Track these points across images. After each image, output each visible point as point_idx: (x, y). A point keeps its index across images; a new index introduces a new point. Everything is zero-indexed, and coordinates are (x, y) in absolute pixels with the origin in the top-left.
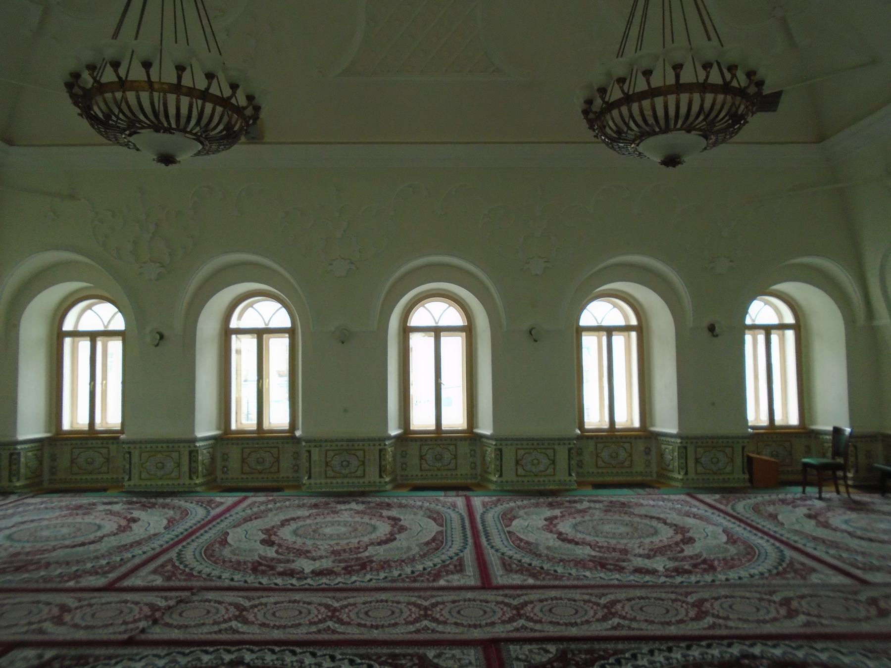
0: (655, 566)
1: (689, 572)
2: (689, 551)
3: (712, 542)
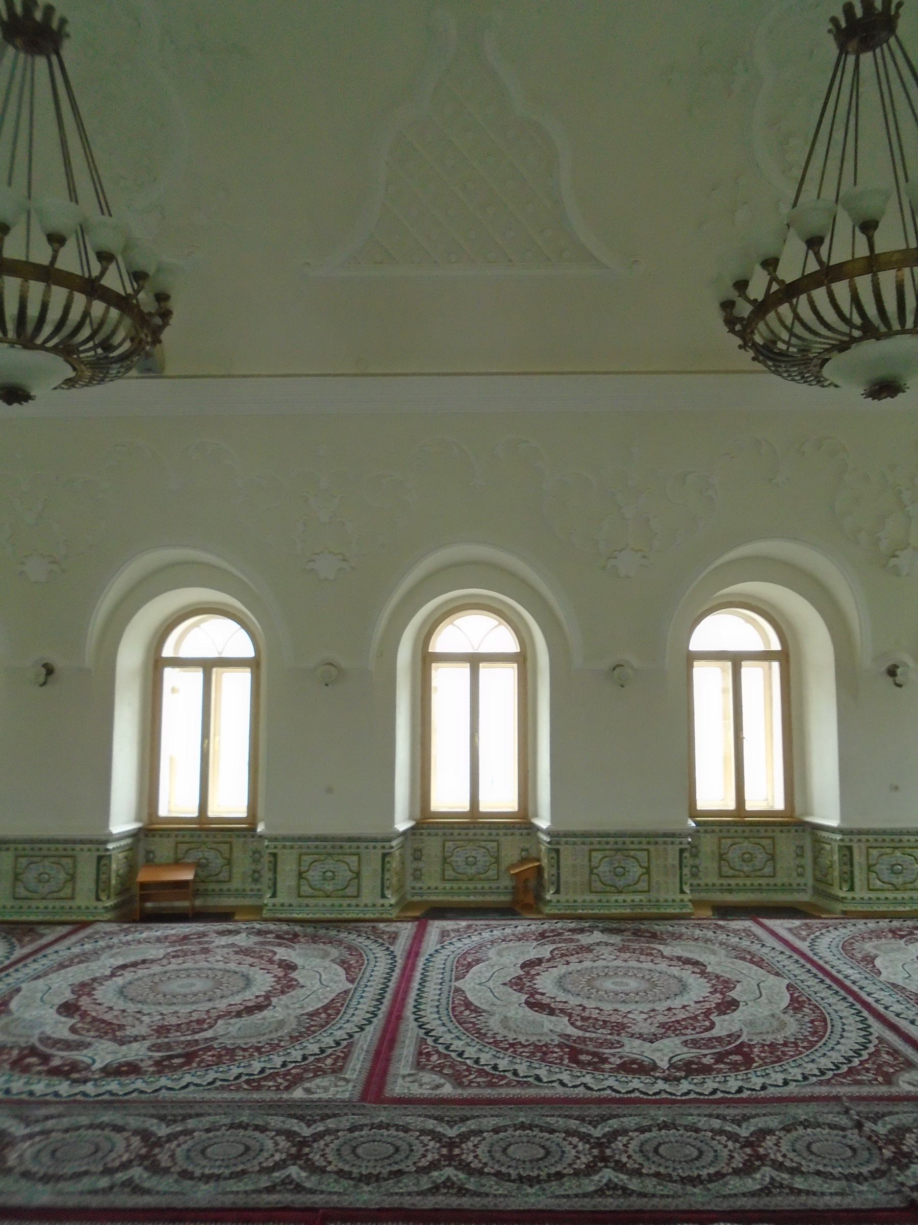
0: (656, 1057)
1: (706, 1070)
2: (723, 1025)
3: (762, 1011)
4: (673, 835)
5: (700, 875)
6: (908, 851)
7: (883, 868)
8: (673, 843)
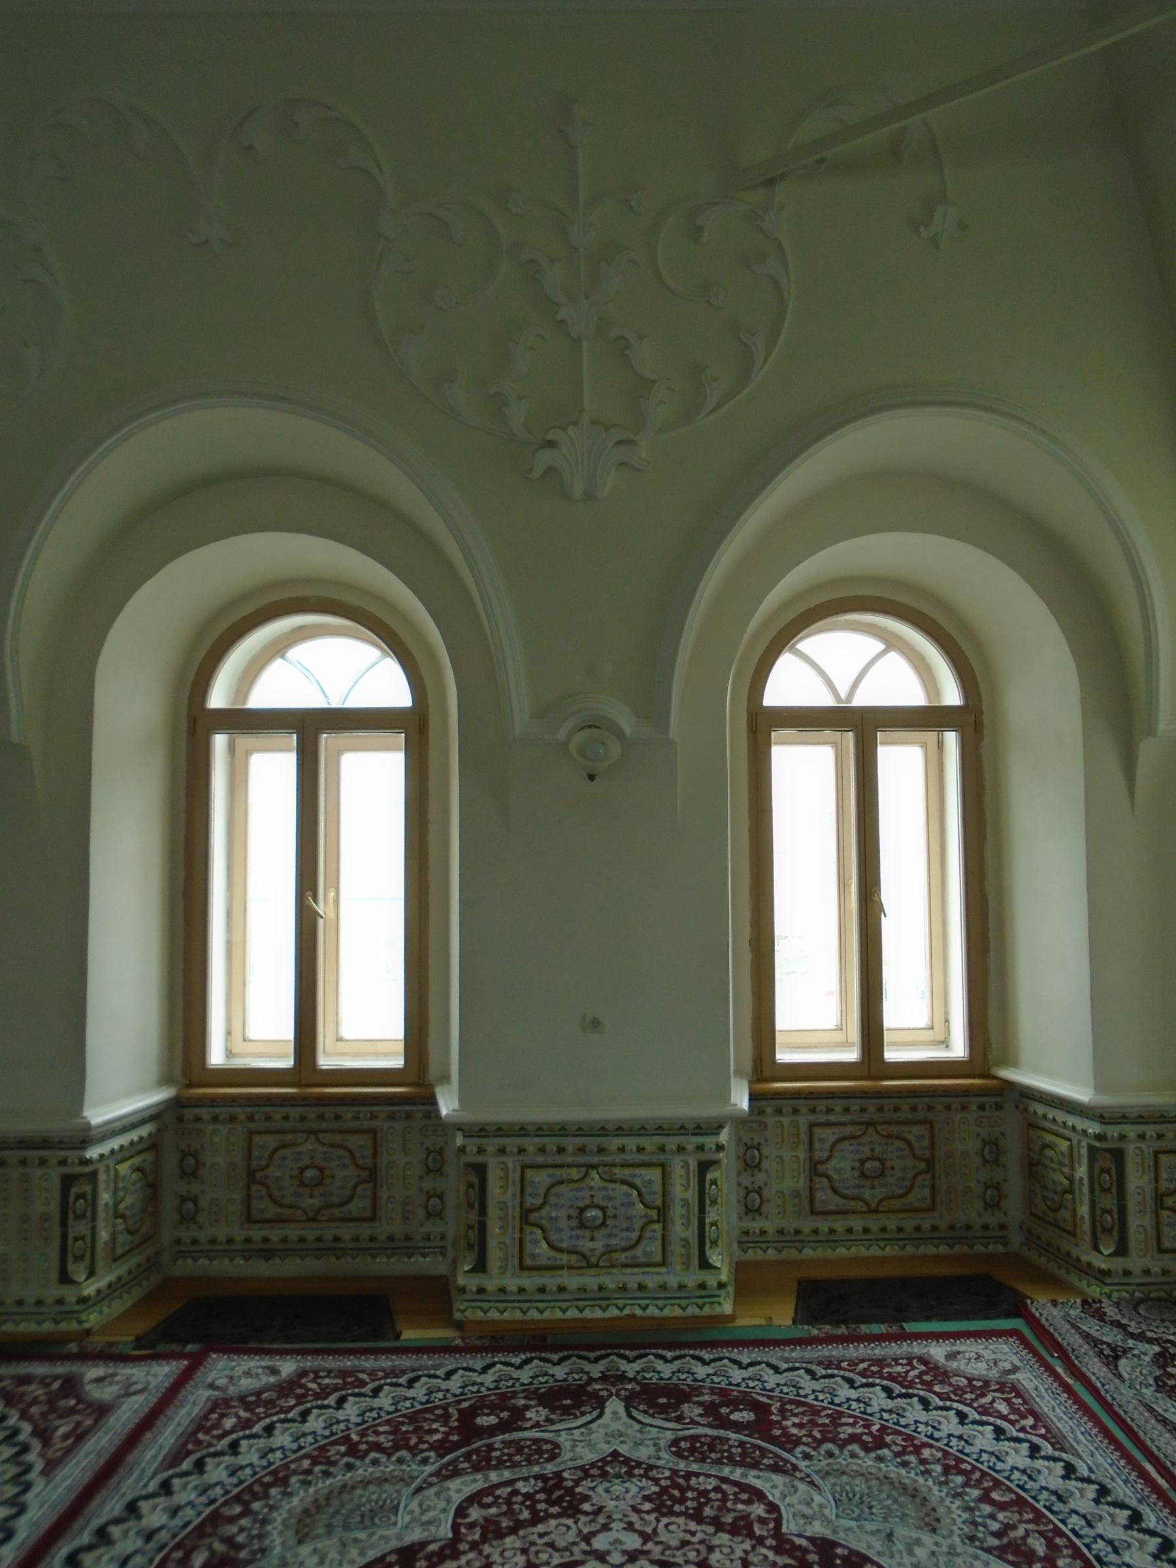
4: (45, 1144)
5: (202, 1218)
6: (620, 1173)
7: (558, 1213)
8: (43, 1162)
